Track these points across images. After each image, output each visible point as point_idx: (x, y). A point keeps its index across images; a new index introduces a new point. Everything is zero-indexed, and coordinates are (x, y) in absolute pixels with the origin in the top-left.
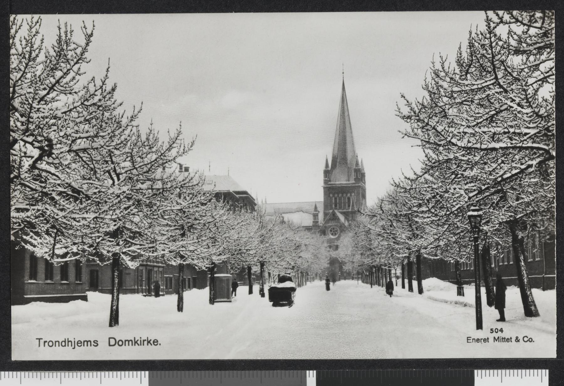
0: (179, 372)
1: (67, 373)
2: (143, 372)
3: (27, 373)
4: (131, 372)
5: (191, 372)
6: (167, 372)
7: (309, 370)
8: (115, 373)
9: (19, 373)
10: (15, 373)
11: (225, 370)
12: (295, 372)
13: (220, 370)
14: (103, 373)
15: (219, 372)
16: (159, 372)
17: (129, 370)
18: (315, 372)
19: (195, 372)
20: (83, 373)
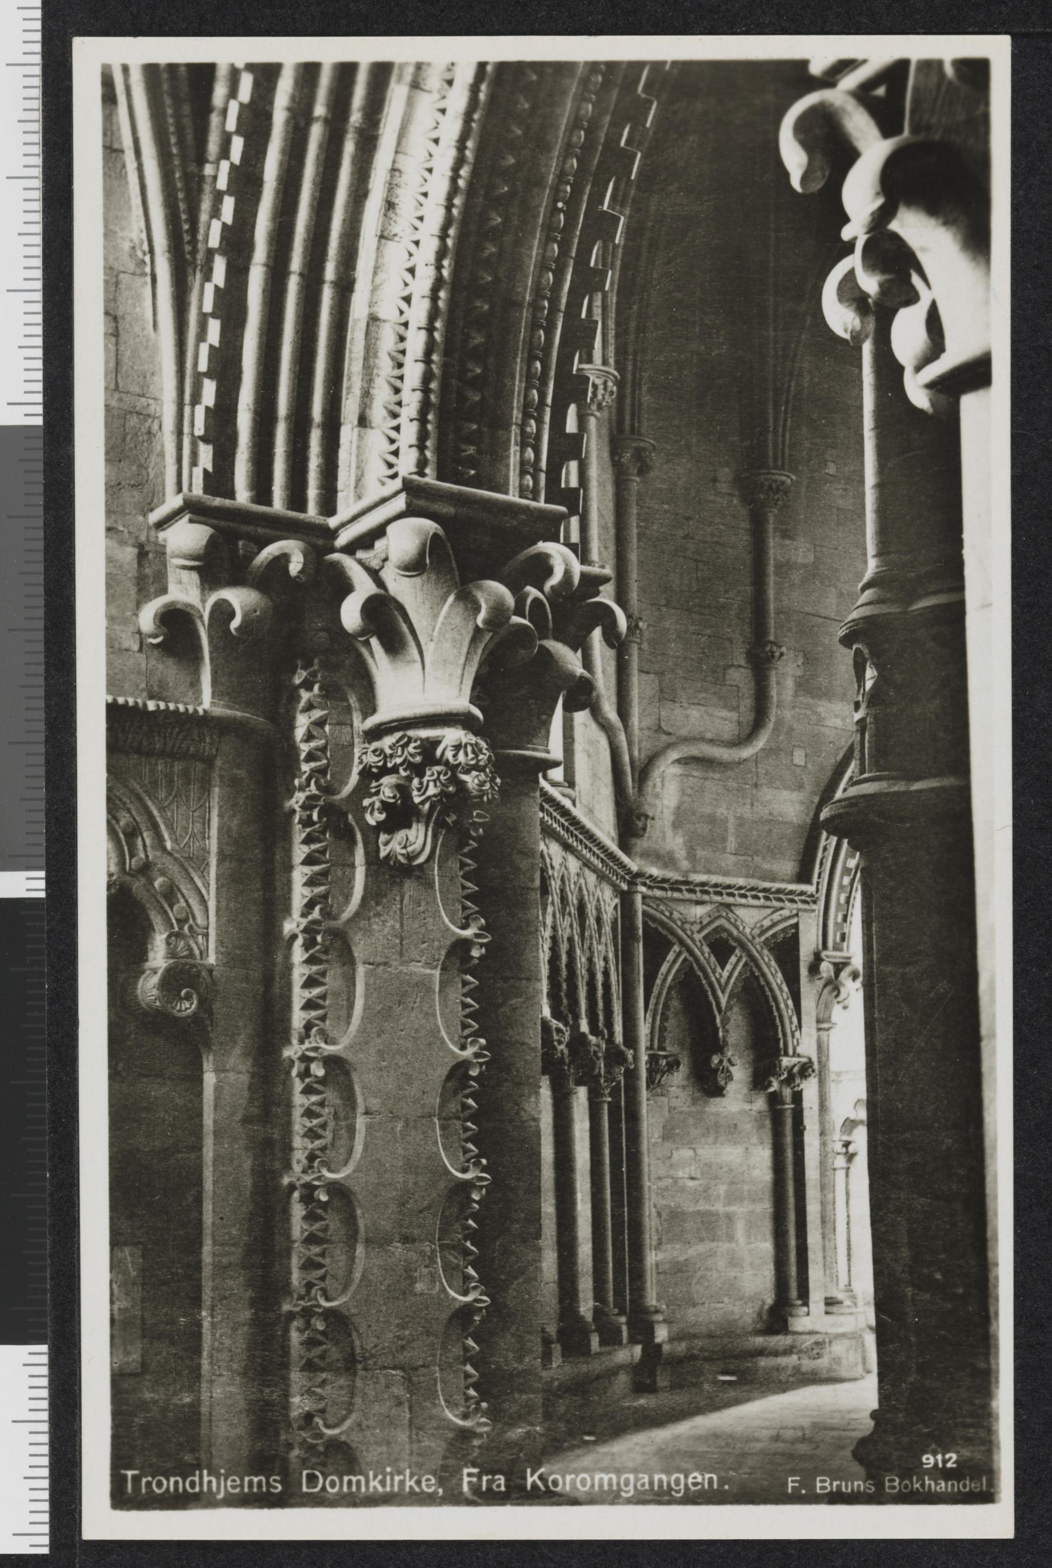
0: (40, 511)
1: (38, 195)
2: (40, 409)
3: (37, 82)
4: (40, 375)
5: (41, 545)
6: (40, 477)
7: (48, 880)
8: (39, 330)
9: (38, 59)
10: (38, 48)
11: (47, 642)
12: (42, 839)
13: (46, 628)
14: (39, 296)
15: (41, 624)
16: (40, 455)
17: (44, 370)
18: (42, 895)
19: (40, 556)
20: (38, 240)
